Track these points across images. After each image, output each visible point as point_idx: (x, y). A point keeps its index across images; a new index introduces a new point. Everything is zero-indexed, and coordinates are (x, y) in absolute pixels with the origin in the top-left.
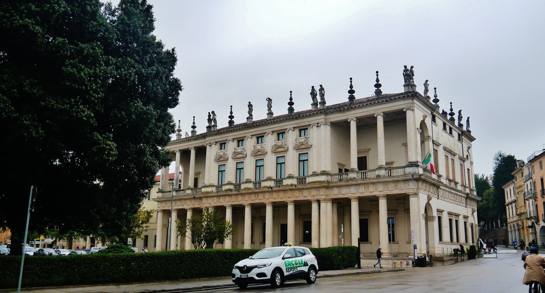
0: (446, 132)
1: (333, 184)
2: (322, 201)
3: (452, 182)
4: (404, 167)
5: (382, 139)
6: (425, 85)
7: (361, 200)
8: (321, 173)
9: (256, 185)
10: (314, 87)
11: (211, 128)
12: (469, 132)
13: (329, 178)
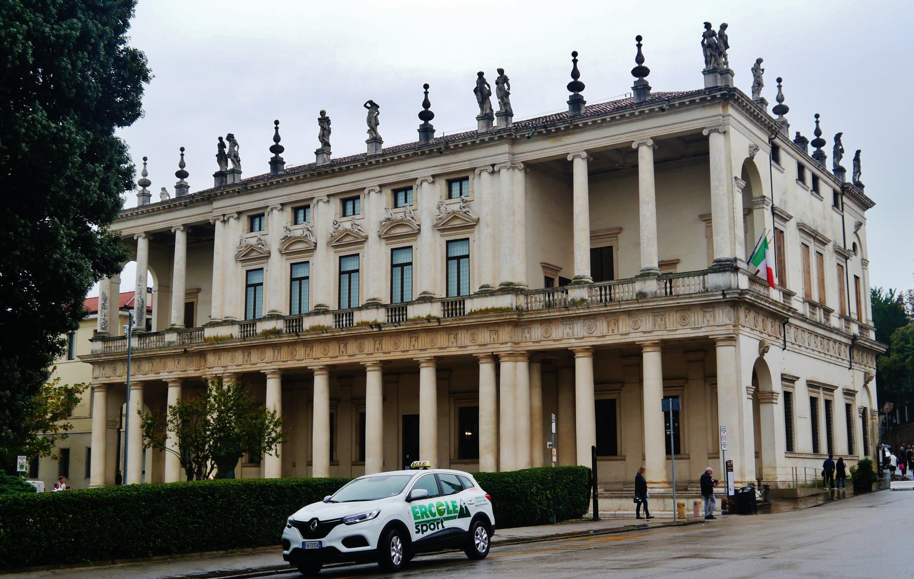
0: (803, 188)
1: (531, 314)
2: (504, 356)
3: (817, 308)
4: (704, 273)
5: (650, 204)
6: (756, 71)
7: (599, 354)
8: (502, 289)
9: (341, 319)
10: (483, 73)
11: (226, 177)
12: (860, 186)
13: (521, 301)
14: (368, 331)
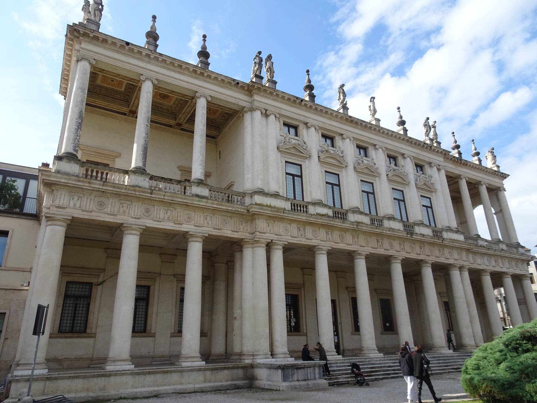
14: (404, 235)
